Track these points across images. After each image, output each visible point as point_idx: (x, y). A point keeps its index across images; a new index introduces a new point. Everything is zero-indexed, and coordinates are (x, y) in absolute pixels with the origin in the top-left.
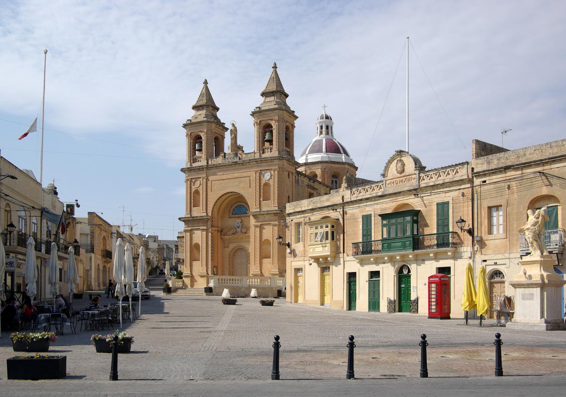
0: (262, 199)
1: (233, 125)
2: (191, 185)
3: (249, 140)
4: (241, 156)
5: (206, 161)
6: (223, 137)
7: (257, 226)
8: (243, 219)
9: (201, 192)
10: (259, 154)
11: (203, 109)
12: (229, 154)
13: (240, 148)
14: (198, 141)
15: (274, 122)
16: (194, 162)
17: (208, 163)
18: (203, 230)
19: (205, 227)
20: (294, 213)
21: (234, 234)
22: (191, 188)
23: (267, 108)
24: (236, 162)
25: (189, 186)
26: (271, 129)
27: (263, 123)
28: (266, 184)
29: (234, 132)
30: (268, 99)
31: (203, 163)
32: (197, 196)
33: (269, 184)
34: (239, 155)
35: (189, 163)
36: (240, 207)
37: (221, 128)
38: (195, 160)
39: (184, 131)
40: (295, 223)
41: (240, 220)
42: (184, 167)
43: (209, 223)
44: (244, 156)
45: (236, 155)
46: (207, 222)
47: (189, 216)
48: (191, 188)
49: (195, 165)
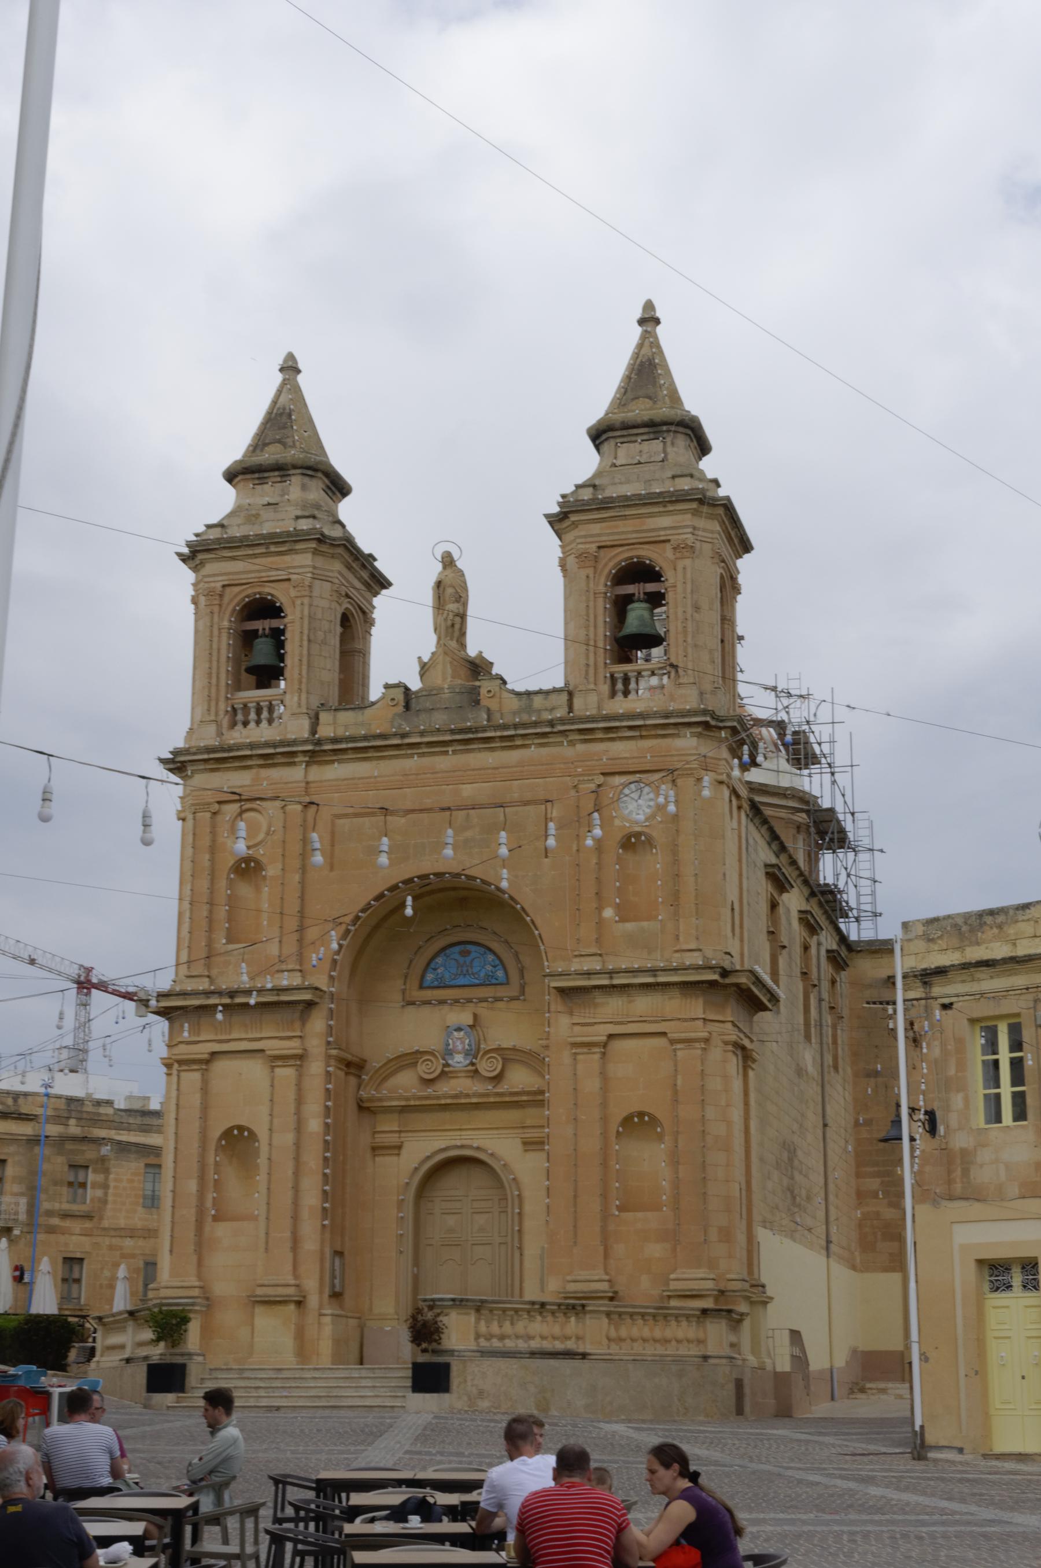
0: (608, 913)
1: (448, 561)
2: (213, 833)
3: (530, 632)
4: (493, 704)
5: (306, 723)
6: (369, 622)
7: (589, 1045)
8: (482, 1010)
9: (272, 870)
10: (593, 698)
11: (262, 481)
12: (428, 692)
13: (478, 668)
14: (262, 625)
15: (669, 553)
16: (233, 725)
17: (314, 732)
18: (277, 1060)
19: (292, 1047)
20: (965, 966)
21: (429, 1082)
22: (213, 849)
23: (628, 490)
24: (476, 730)
25: (206, 841)
26: (651, 587)
27: (613, 560)
28: (633, 842)
29: (450, 598)
30: (626, 452)
31: (298, 728)
32: (245, 890)
33: (650, 842)
34: (485, 702)
35: (212, 729)
36: (465, 953)
37: (365, 575)
38: (238, 716)
39: (187, 576)
40: (973, 1021)
41: (465, 1018)
42: (181, 744)
43: (318, 1023)
44: (515, 704)
45: (473, 698)
46: (304, 1019)
47: (203, 985)
48: (213, 849)
49: (239, 736)
